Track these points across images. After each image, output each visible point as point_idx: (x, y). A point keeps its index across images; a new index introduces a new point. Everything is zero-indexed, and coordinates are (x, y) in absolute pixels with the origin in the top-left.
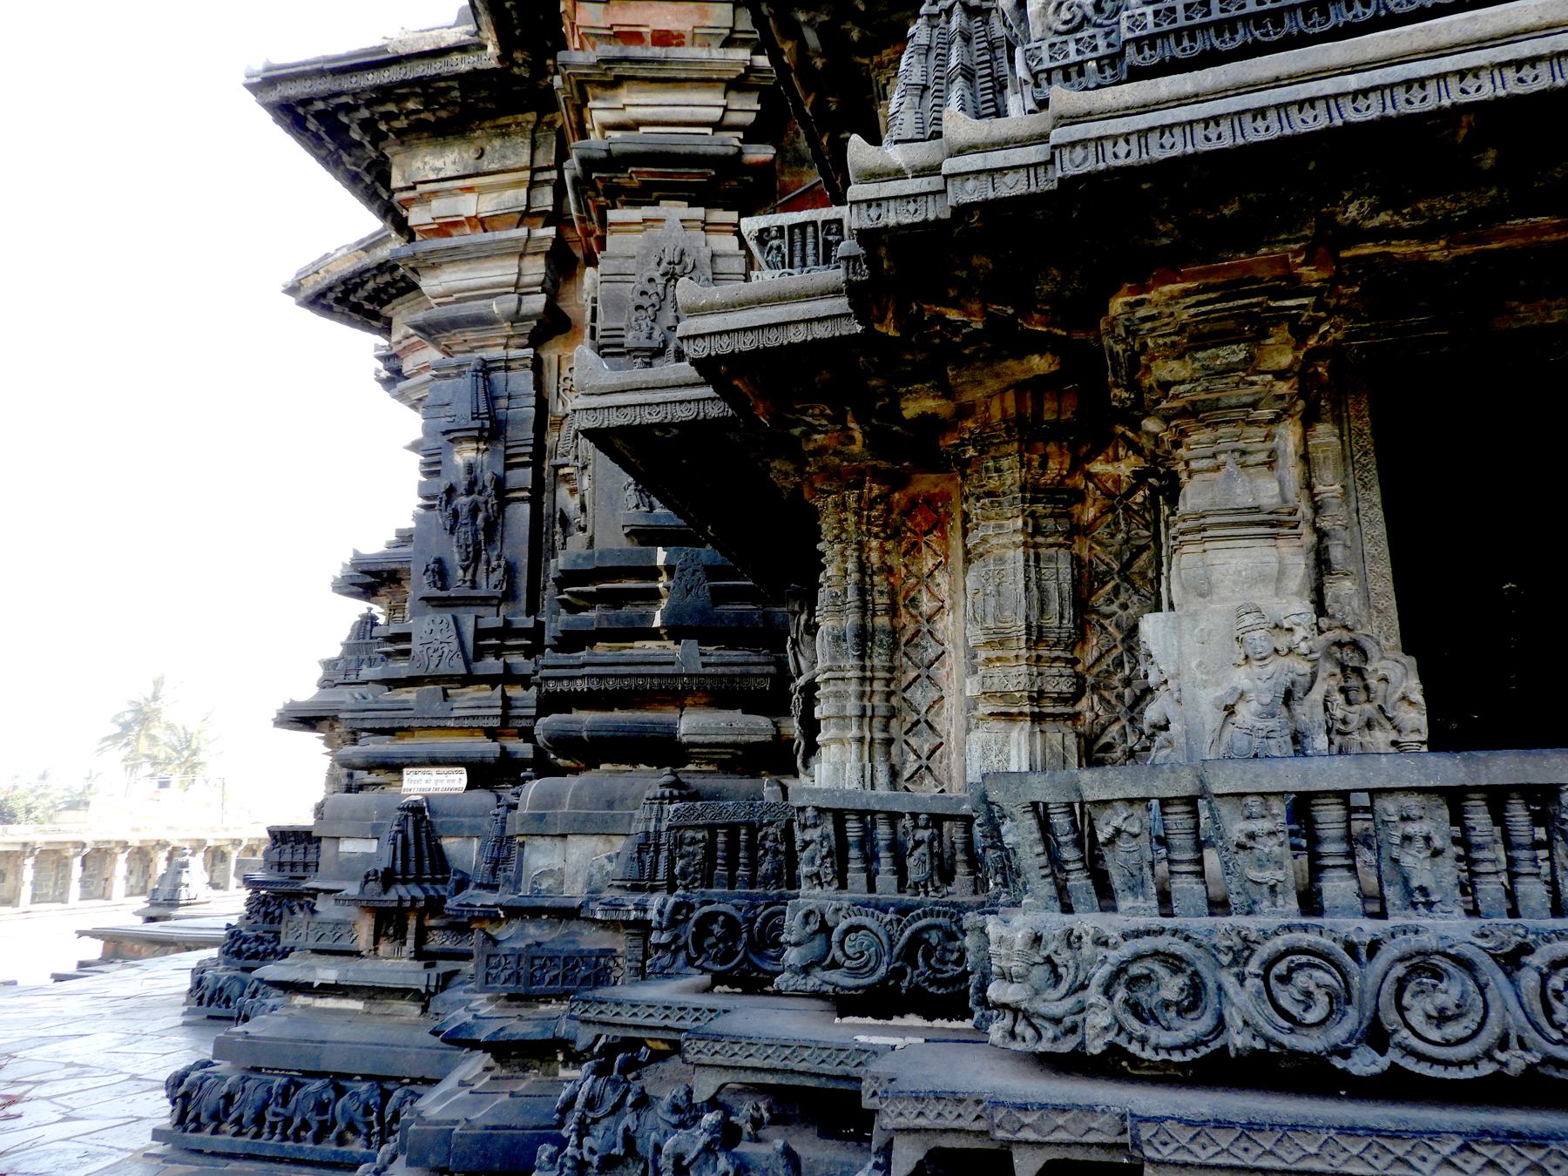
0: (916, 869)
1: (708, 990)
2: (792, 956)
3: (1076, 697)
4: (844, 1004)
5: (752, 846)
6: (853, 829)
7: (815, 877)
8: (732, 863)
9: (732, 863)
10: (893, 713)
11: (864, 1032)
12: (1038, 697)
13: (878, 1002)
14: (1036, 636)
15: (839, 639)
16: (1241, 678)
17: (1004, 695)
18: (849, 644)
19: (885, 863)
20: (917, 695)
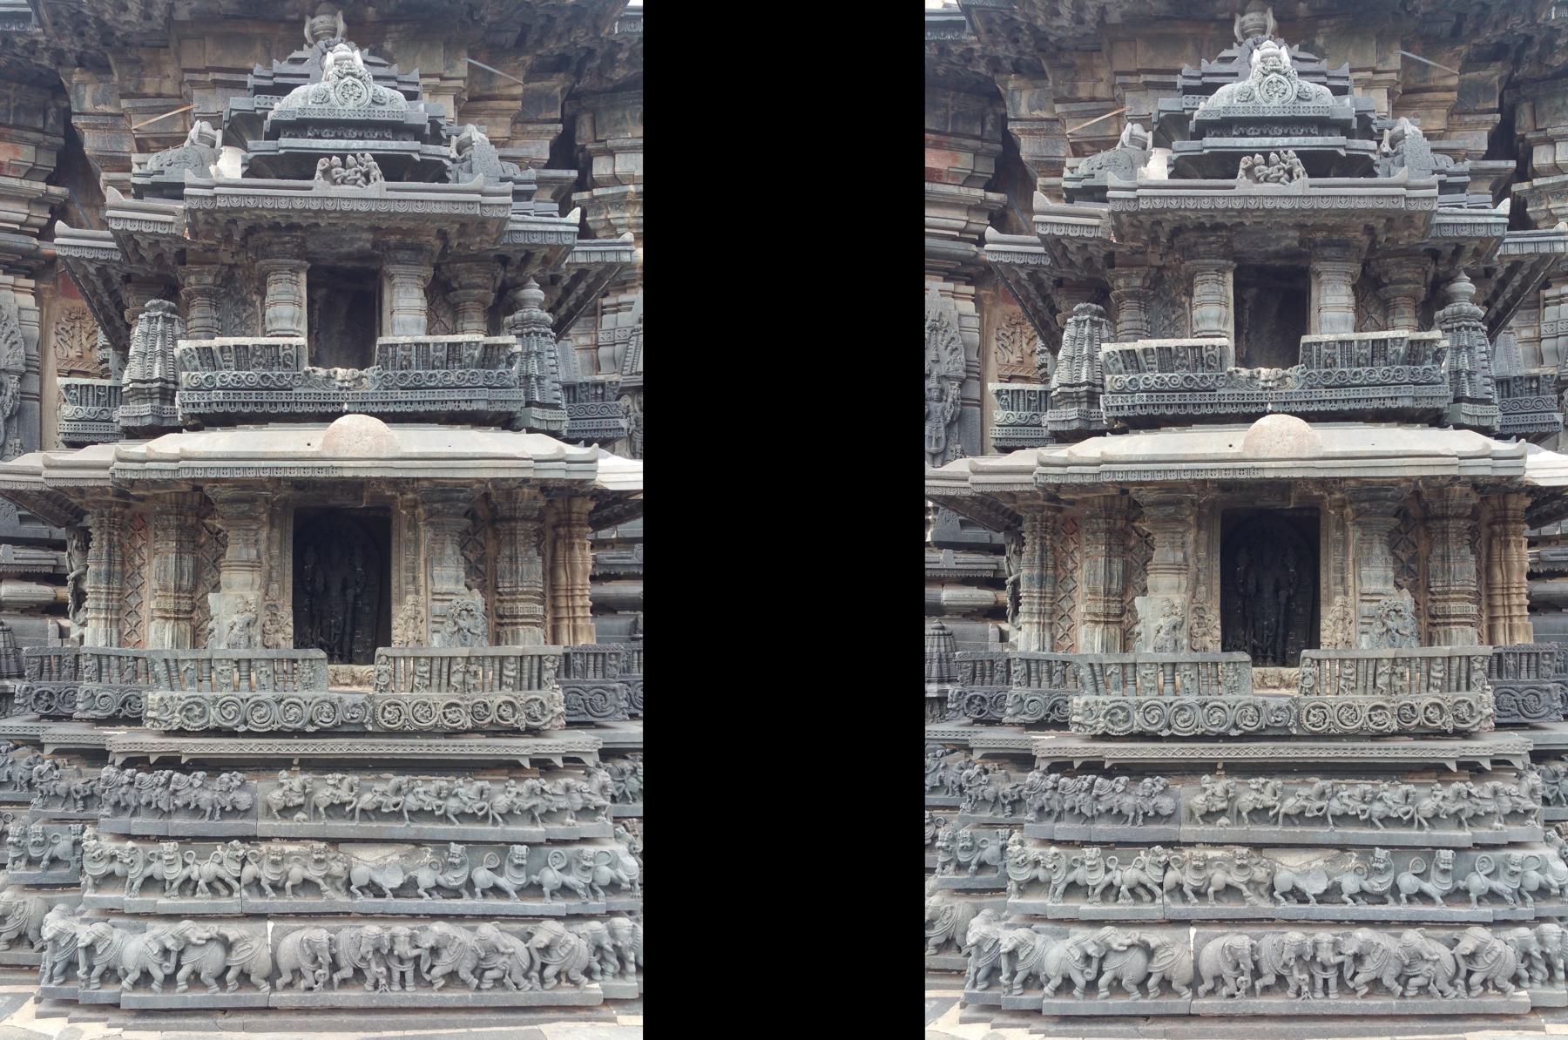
0: (1056, 679)
1: (971, 725)
2: (1009, 711)
3: (1121, 615)
4: (1029, 727)
5: (992, 668)
6: (1033, 666)
7: (1019, 683)
8: (983, 676)
9: (983, 676)
10: (1053, 613)
11: (1035, 736)
12: (1107, 615)
13: (1041, 725)
14: (1108, 592)
15: (1030, 579)
16: (1162, 621)
17: (1096, 615)
18: (1035, 582)
19: (1044, 677)
20: (1066, 605)
